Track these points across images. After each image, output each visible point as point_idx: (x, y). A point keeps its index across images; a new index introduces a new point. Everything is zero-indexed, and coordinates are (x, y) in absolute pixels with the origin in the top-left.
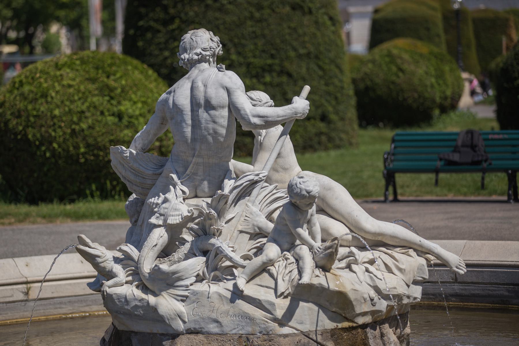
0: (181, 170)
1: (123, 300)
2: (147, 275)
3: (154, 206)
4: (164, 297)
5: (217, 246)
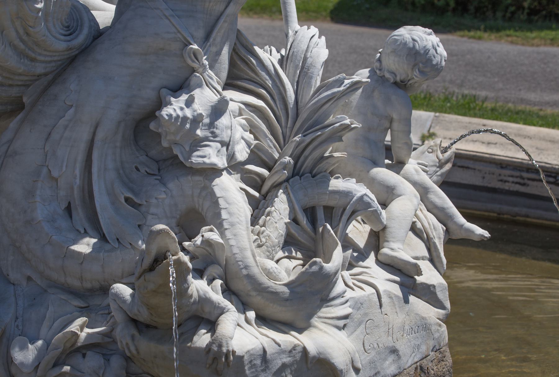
0: (200, 34)
1: (258, 362)
2: (286, 290)
3: (188, 126)
4: (321, 330)
5: (359, 195)
